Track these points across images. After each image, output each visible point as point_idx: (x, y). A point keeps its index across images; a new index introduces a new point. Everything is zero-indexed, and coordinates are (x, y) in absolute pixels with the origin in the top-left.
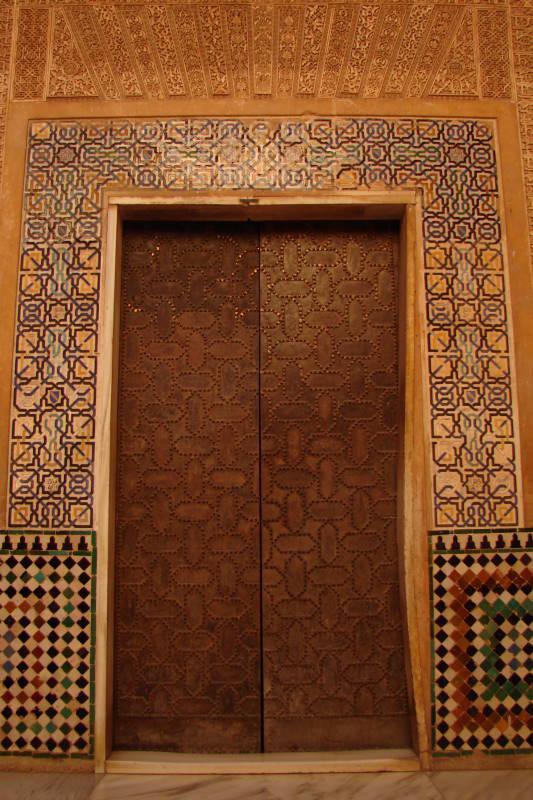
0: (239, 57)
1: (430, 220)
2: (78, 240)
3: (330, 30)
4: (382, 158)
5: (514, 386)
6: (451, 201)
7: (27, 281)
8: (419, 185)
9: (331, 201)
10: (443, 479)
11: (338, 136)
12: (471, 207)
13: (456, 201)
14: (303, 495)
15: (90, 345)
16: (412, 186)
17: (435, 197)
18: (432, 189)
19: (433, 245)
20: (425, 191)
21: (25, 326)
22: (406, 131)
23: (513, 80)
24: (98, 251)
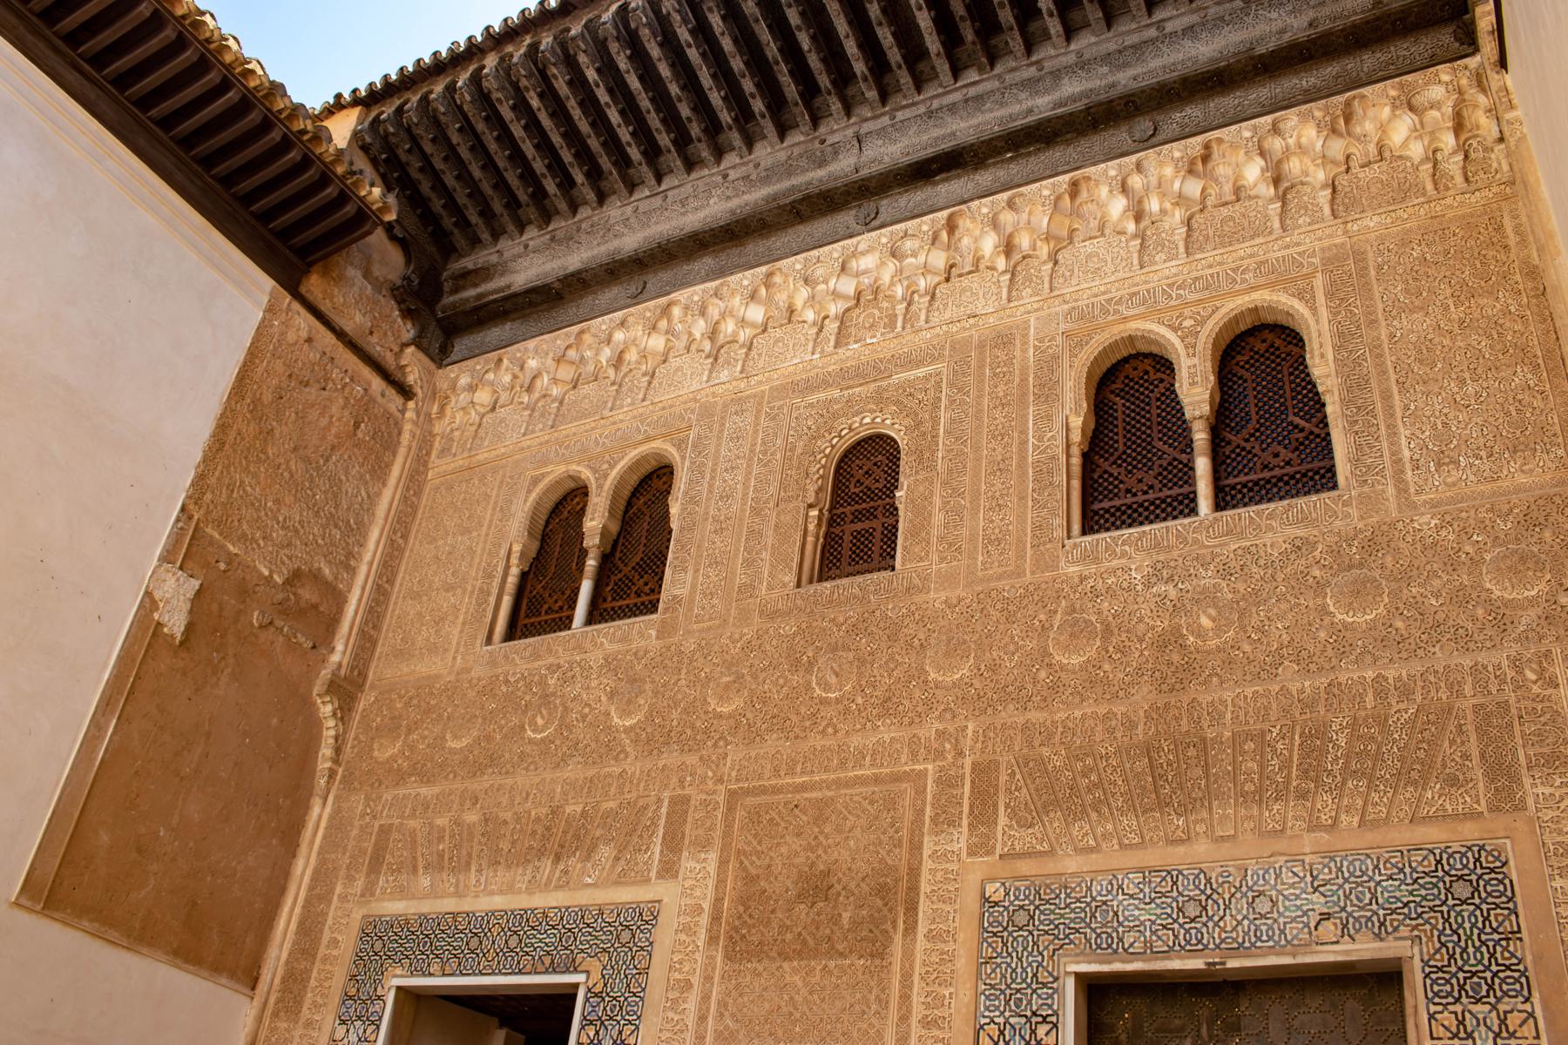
0: (1197, 794)
1: (1434, 976)
2: (1034, 1014)
3: (1295, 753)
4: (1367, 901)
6: (1458, 950)
8: (1416, 933)
9: (1308, 959)
11: (1314, 878)
12: (1486, 956)
13: (1464, 950)
16: (1407, 934)
17: (1438, 945)
18: (1432, 935)
19: (1440, 1008)
20: (1424, 939)
22: (1394, 866)
23: (1527, 786)
24: (1055, 1026)
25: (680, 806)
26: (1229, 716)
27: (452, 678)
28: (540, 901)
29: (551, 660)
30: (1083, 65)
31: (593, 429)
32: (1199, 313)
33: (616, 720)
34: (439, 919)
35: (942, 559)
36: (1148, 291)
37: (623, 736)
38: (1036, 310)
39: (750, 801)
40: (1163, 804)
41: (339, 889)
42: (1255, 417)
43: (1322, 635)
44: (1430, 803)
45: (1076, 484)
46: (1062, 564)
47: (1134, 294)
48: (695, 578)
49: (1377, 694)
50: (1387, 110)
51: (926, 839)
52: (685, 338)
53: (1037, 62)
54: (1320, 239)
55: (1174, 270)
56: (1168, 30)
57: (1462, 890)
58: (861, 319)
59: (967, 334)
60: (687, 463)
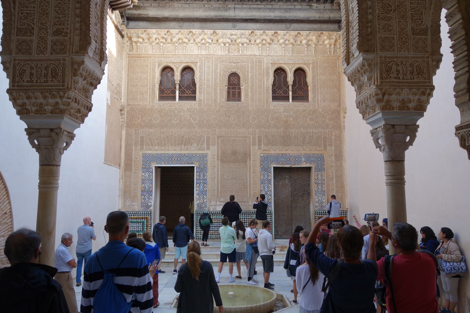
5: (326, 192)
7: (262, 177)
10: (316, 204)
14: (297, 205)
15: (270, 186)
21: (262, 183)
25: (208, 138)
27: (150, 107)
28: (183, 152)
29: (175, 107)
30: (280, 9)
31: (173, 56)
33: (192, 121)
35: (251, 102)
41: (134, 148)
42: (297, 85)
45: (272, 92)
47: (283, 59)
48: (204, 96)
50: (325, 37)
51: (251, 147)
52: (193, 40)
53: (272, 5)
56: (296, 8)
57: (319, 159)
58: (232, 48)
60: (198, 71)
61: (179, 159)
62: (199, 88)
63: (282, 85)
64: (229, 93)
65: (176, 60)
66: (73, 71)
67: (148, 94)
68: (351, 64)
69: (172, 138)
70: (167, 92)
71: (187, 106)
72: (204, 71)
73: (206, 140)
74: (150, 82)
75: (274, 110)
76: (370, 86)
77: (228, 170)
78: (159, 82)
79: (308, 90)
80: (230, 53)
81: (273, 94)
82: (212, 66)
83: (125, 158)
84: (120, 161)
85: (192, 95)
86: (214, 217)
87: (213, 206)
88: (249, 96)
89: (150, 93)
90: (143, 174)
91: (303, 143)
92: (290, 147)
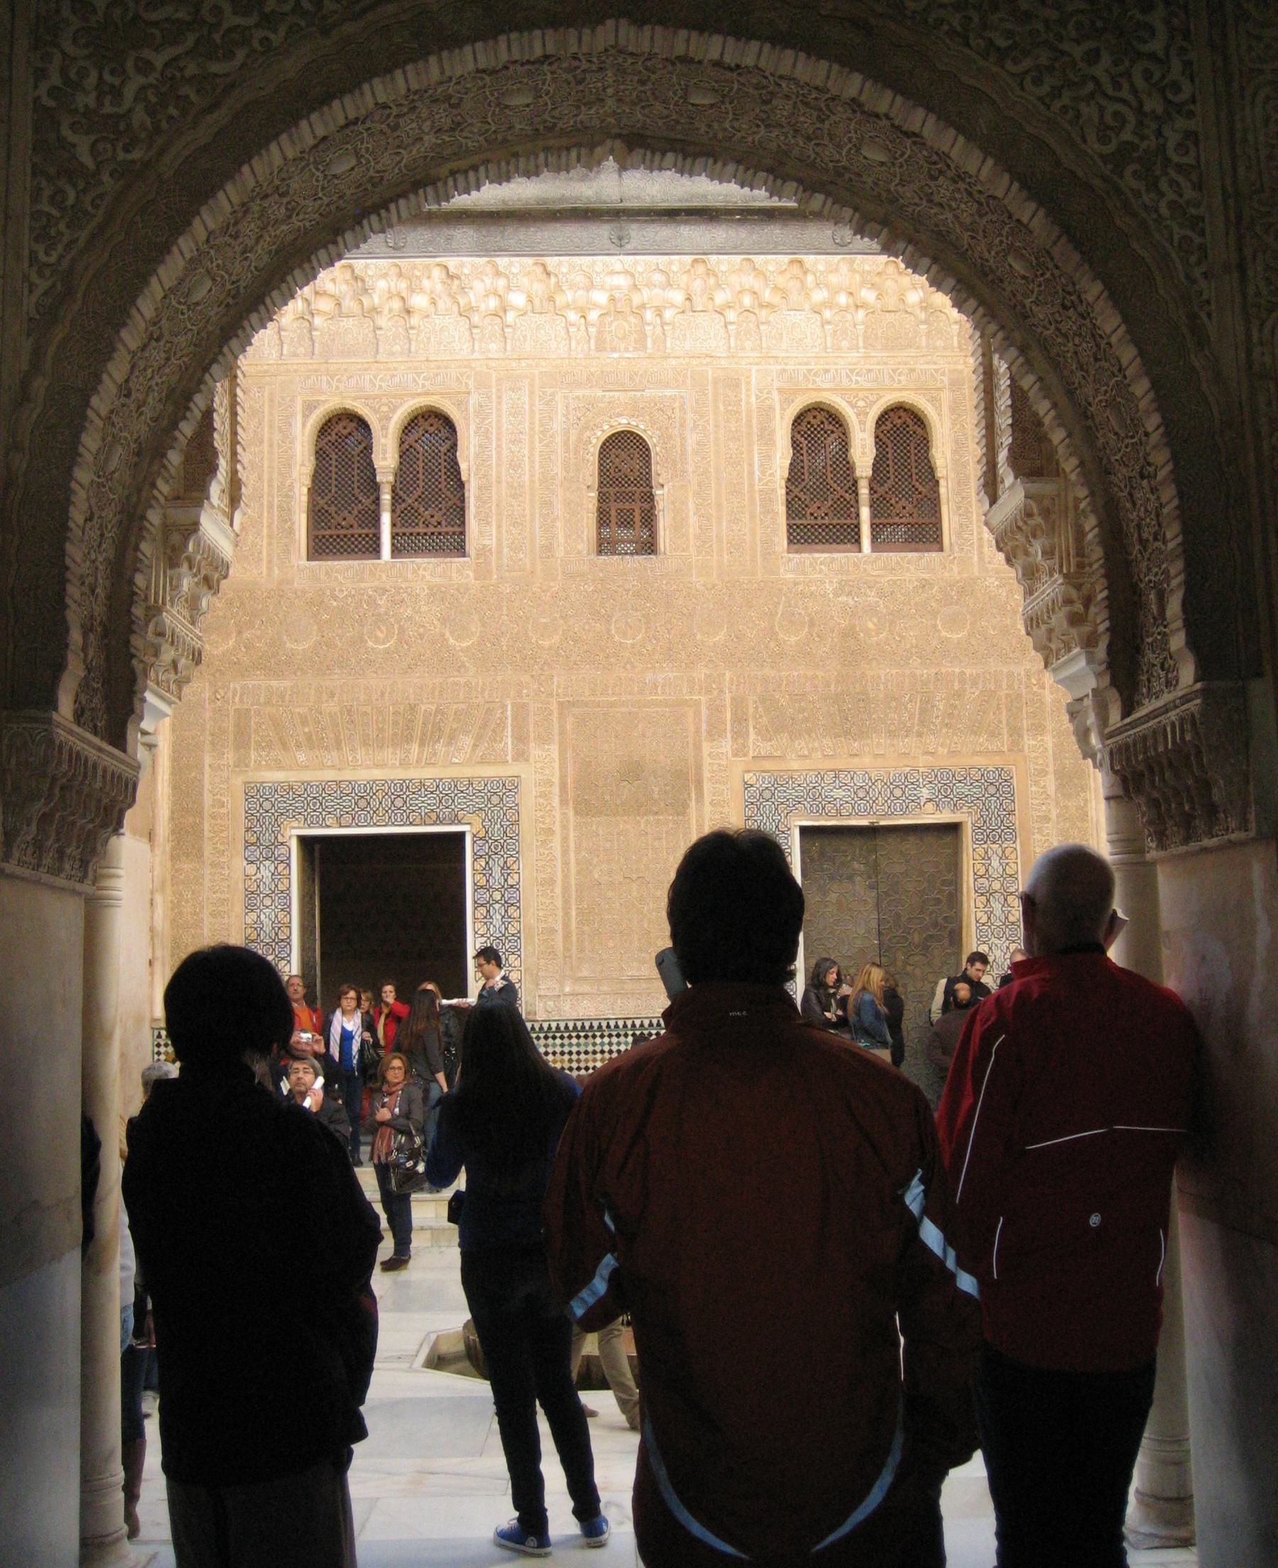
25: (521, 711)
26: (882, 687)
29: (376, 584)
31: (366, 370)
32: (867, 397)
33: (451, 641)
34: (324, 786)
35: (699, 553)
36: (836, 370)
37: (461, 654)
38: (757, 364)
39: (575, 710)
40: (847, 733)
41: (208, 760)
42: (892, 477)
43: (935, 643)
44: (981, 745)
46: (782, 571)
47: (827, 371)
48: (499, 532)
49: (959, 682)
51: (705, 744)
54: (949, 363)
55: (854, 360)
57: (992, 790)
58: (613, 328)
59: (704, 368)
60: (473, 427)
61: (399, 803)
62: (478, 498)
63: (829, 480)
64: (603, 518)
65: (380, 387)
66: (168, 551)
67: (265, 530)
68: (1000, 501)
69: (366, 713)
70: (339, 519)
71: (428, 578)
72: (499, 428)
73: (515, 719)
74: (270, 480)
75: (796, 584)
76: (1051, 576)
77: (608, 845)
78: (307, 481)
79: (937, 498)
80: (604, 349)
81: (789, 516)
82: (532, 405)
83: (174, 803)
84: (154, 817)
85: (450, 529)
86: (554, 1046)
87: (550, 998)
88: (691, 530)
89: (270, 526)
90: (251, 869)
91: (922, 722)
92: (869, 741)
